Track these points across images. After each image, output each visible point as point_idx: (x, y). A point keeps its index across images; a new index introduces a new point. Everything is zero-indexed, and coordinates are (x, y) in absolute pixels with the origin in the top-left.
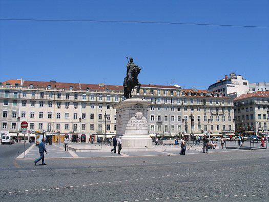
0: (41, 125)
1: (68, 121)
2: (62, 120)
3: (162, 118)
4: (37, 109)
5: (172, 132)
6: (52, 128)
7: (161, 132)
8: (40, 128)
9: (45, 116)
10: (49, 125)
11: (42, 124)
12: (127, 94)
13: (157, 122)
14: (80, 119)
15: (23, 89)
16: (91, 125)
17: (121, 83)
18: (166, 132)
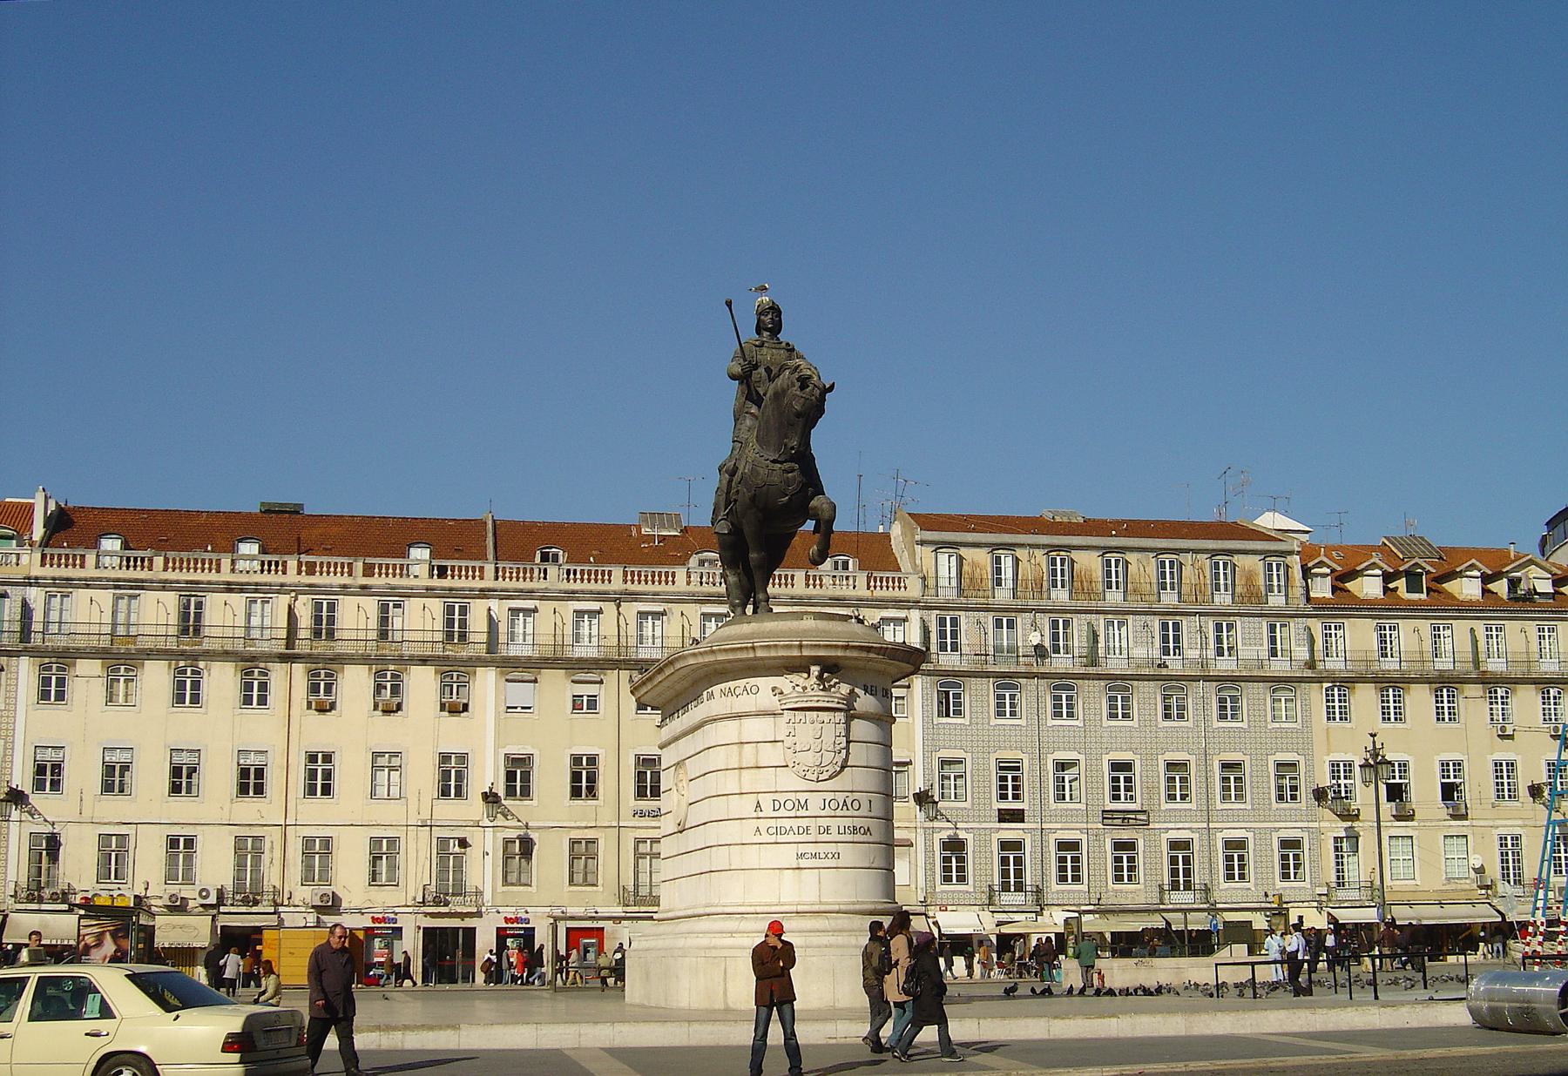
0: (180, 847)
1: (389, 813)
2: (349, 815)
3: (1149, 777)
4: (148, 720)
5: (1226, 892)
6: (271, 877)
7: (1136, 892)
8: (170, 877)
9: (218, 777)
10: (248, 850)
11: (190, 842)
12: (749, 583)
13: (1107, 815)
14: (490, 798)
15: (48, 571)
16: (574, 842)
17: (700, 508)
18: (1182, 898)
